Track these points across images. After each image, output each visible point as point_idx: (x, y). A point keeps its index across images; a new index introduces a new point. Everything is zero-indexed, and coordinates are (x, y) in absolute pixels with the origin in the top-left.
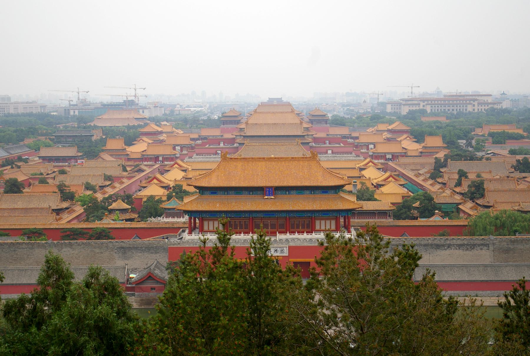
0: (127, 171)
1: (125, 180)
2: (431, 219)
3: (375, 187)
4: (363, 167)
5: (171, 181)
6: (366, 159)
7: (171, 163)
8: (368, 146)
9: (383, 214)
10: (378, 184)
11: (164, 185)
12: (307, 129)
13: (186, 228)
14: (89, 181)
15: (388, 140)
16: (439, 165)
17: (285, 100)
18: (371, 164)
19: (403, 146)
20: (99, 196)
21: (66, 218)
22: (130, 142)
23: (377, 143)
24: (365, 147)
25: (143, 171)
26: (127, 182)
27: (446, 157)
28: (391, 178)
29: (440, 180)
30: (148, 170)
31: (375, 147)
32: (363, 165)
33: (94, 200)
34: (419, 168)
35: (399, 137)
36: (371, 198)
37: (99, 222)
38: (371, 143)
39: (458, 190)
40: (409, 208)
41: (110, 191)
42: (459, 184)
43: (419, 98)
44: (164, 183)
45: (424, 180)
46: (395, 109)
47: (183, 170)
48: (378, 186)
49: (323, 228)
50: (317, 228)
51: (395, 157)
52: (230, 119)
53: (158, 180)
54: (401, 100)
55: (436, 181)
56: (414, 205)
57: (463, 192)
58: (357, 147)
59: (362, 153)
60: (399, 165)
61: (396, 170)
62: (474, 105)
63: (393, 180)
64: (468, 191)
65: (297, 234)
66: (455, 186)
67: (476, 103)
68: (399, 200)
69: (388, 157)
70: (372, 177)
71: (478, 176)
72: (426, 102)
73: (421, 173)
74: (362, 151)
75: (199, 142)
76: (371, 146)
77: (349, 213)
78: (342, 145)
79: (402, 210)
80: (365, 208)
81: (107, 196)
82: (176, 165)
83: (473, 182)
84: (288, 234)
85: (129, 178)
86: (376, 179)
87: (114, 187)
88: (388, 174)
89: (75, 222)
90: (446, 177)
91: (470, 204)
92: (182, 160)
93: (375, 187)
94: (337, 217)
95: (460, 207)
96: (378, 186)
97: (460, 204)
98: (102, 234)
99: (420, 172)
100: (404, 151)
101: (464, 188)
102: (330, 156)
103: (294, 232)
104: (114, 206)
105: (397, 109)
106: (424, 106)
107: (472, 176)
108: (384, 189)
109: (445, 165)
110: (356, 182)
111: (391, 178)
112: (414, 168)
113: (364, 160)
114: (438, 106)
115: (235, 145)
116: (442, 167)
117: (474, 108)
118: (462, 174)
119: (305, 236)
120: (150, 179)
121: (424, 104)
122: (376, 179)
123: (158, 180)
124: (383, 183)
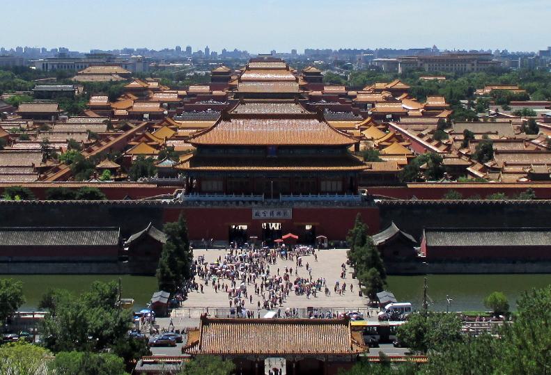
0: (113, 128)
1: (112, 138)
3: (377, 147)
5: (160, 139)
6: (365, 118)
11: (154, 143)
12: (301, 87)
15: (386, 98)
16: (442, 125)
20: (87, 155)
21: (52, 176)
22: (113, 99)
23: (377, 102)
25: (131, 128)
26: (113, 141)
27: (449, 117)
28: (394, 139)
29: (445, 142)
30: (135, 128)
34: (421, 127)
36: (376, 159)
38: (369, 103)
40: (417, 170)
41: (97, 150)
42: (465, 146)
47: (172, 129)
48: (381, 147)
51: (396, 117)
65: (301, 196)
67: (475, 62)
70: (375, 138)
79: (411, 170)
81: (94, 154)
85: (116, 136)
87: (100, 145)
88: (390, 134)
90: (451, 137)
91: (479, 166)
92: (171, 117)
93: (377, 147)
95: (469, 169)
96: (381, 147)
97: (468, 166)
99: (424, 133)
100: (405, 111)
104: (101, 165)
108: (386, 150)
109: (449, 125)
113: (363, 120)
118: (469, 137)
121: (421, 62)
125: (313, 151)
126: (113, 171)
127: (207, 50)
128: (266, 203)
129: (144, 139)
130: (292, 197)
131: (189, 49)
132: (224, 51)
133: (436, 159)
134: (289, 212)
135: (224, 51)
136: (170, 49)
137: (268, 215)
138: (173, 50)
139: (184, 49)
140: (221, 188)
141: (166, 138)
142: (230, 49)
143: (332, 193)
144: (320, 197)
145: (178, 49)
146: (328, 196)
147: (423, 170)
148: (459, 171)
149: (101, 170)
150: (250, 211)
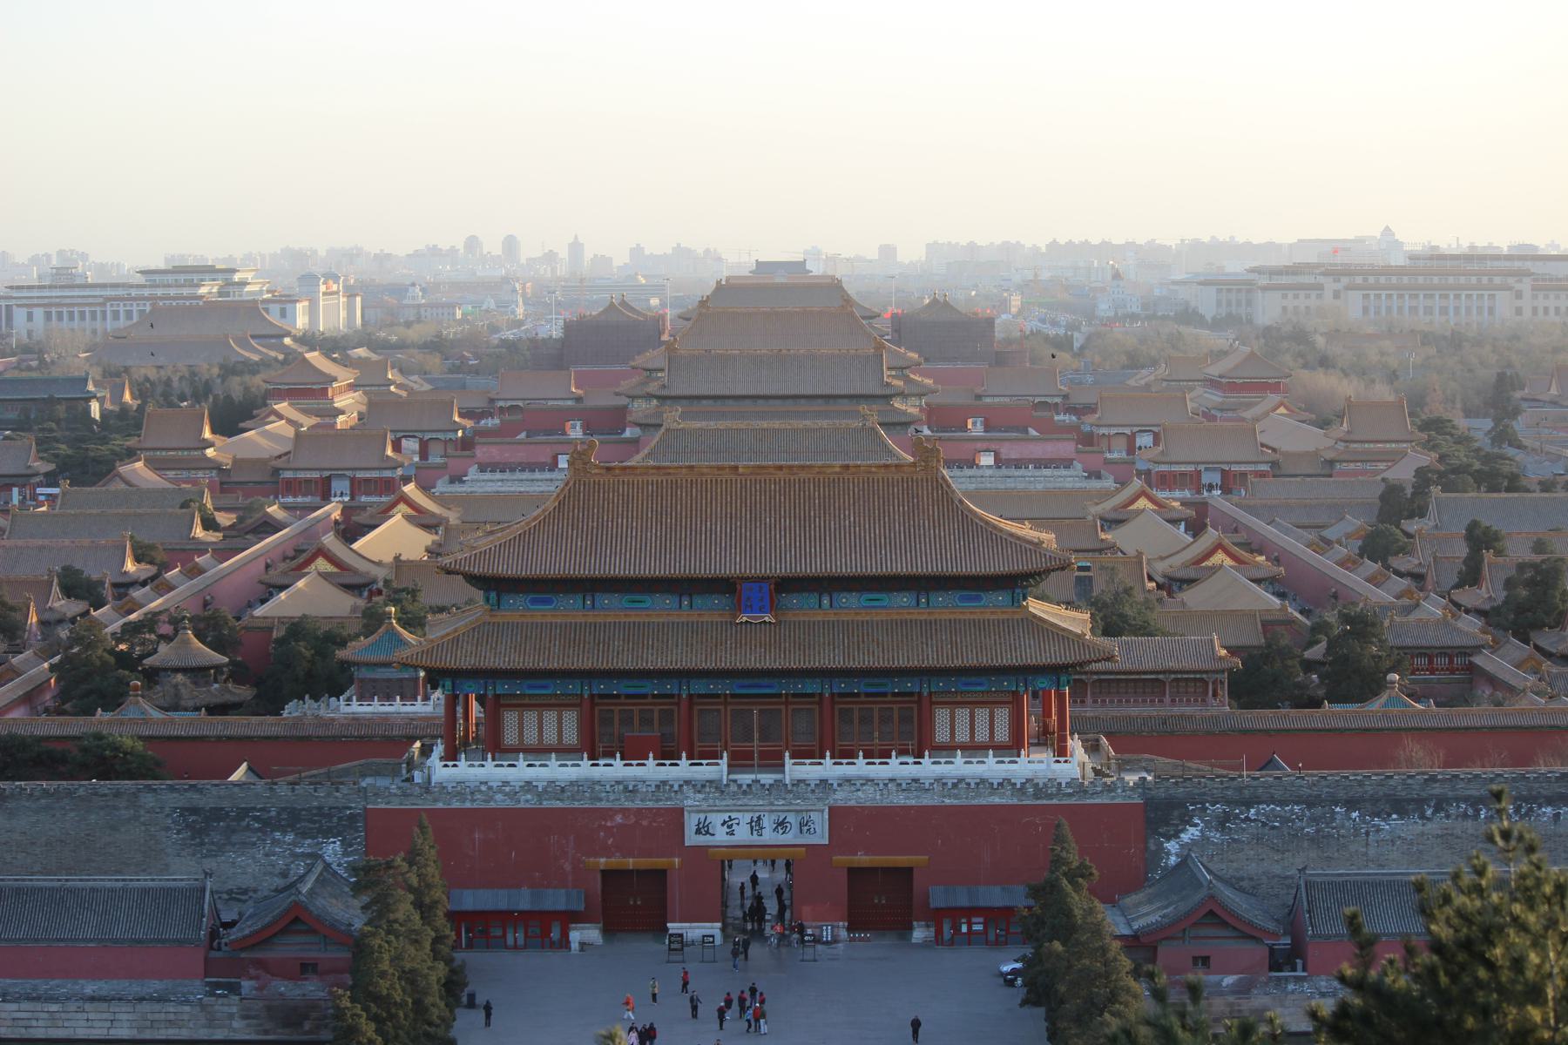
2: (1375, 705)
4: (1113, 516)
6: (1123, 483)
7: (384, 499)
8: (1131, 439)
9: (1192, 683)
10: (1171, 579)
13: (436, 737)
14: (78, 566)
17: (816, 269)
18: (1143, 503)
19: (1260, 438)
24: (1121, 443)
29: (1396, 562)
31: (1156, 442)
32: (1115, 509)
33: (86, 635)
35: (1249, 406)
37: (108, 716)
39: (1467, 597)
43: (1318, 266)
44: (355, 572)
45: (1341, 564)
46: (1229, 304)
48: (1172, 584)
49: (962, 736)
50: (942, 735)
52: (607, 337)
53: (332, 559)
54: (1252, 270)
55: (1388, 567)
56: (1308, 654)
57: (1487, 607)
58: (1088, 440)
59: (1107, 462)
60: (1250, 510)
62: (1519, 295)
63: (1228, 562)
64: (1505, 603)
65: (861, 761)
66: (1457, 586)
68: (1252, 637)
69: (1206, 478)
71: (1539, 547)
72: (1345, 280)
73: (1333, 538)
74: (1108, 456)
75: (491, 423)
76: (1145, 440)
77: (1063, 679)
78: (1033, 432)
80: (1122, 662)
82: (402, 507)
83: (1521, 567)
84: (828, 761)
86: (1162, 558)
89: (17, 714)
92: (425, 488)
94: (1016, 694)
95: (1478, 660)
98: (103, 762)
101: (1488, 593)
102: (989, 472)
103: (849, 754)
105: (1239, 303)
106: (1336, 295)
108: (1192, 598)
110: (1087, 569)
111: (1219, 558)
112: (1306, 521)
113: (1118, 491)
114: (1389, 296)
115: (628, 433)
116: (1411, 516)
117: (1519, 303)
119: (896, 767)
120: (299, 558)
122: (1162, 558)
123: (332, 559)
124: (1192, 574)
125: (905, 599)
126: (198, 673)
127: (576, 247)
128: (733, 788)
129: (322, 564)
131: (510, 244)
132: (637, 251)
133: (1362, 625)
135: (637, 251)
136: (444, 245)
137: (743, 835)
138: (453, 250)
139: (492, 246)
140: (571, 736)
141: (397, 558)
142: (658, 244)
145: (472, 243)
146: (959, 759)
147: (1309, 666)
149: (152, 676)
150: (678, 814)
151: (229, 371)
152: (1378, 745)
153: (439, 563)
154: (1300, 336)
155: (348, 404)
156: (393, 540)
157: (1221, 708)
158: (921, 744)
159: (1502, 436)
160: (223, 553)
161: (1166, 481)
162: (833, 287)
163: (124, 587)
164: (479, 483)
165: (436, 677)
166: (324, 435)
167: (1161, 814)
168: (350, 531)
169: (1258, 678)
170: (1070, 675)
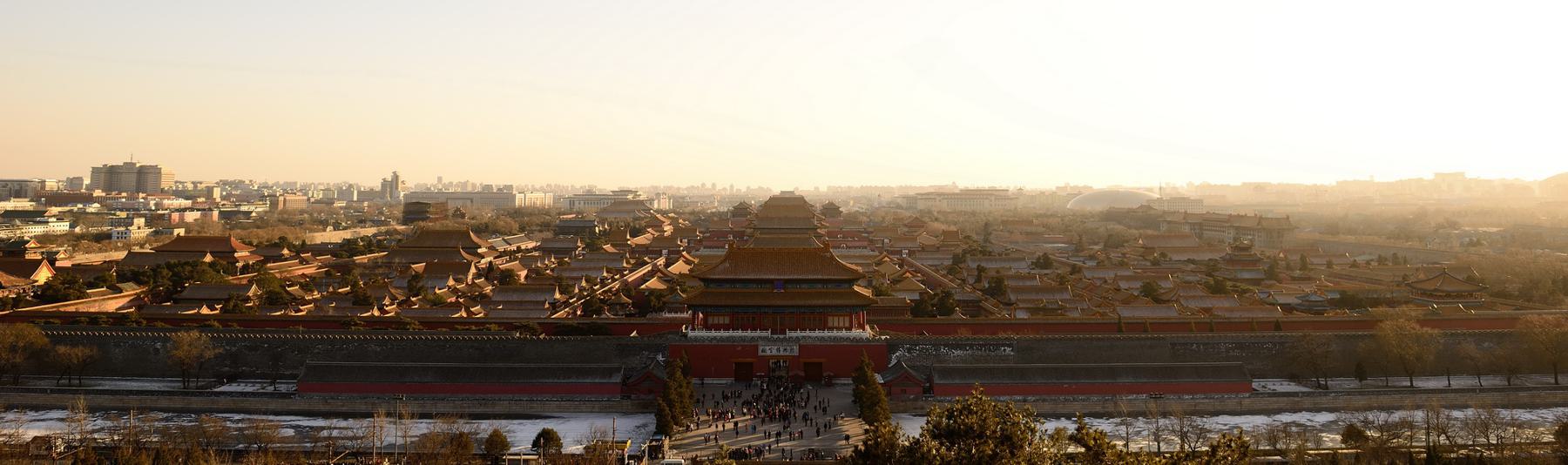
42: (979, 280)
52: (741, 210)
61: (912, 265)
107: (993, 273)
118: (980, 270)
130: (799, 333)
133: (948, 295)
134: (796, 348)
137: (774, 352)
143: (839, 329)
144: (826, 334)
148: (973, 307)
151: (636, 219)
152: (953, 327)
153: (692, 275)
154: (930, 212)
155: (668, 229)
156: (679, 267)
157: (909, 316)
158: (824, 327)
159: (986, 240)
160: (631, 271)
161: (893, 253)
162: (802, 198)
163: (603, 280)
164: (703, 252)
165: (690, 307)
166: (660, 239)
167: (891, 347)
168: (667, 265)
169: (917, 309)
170: (865, 305)
